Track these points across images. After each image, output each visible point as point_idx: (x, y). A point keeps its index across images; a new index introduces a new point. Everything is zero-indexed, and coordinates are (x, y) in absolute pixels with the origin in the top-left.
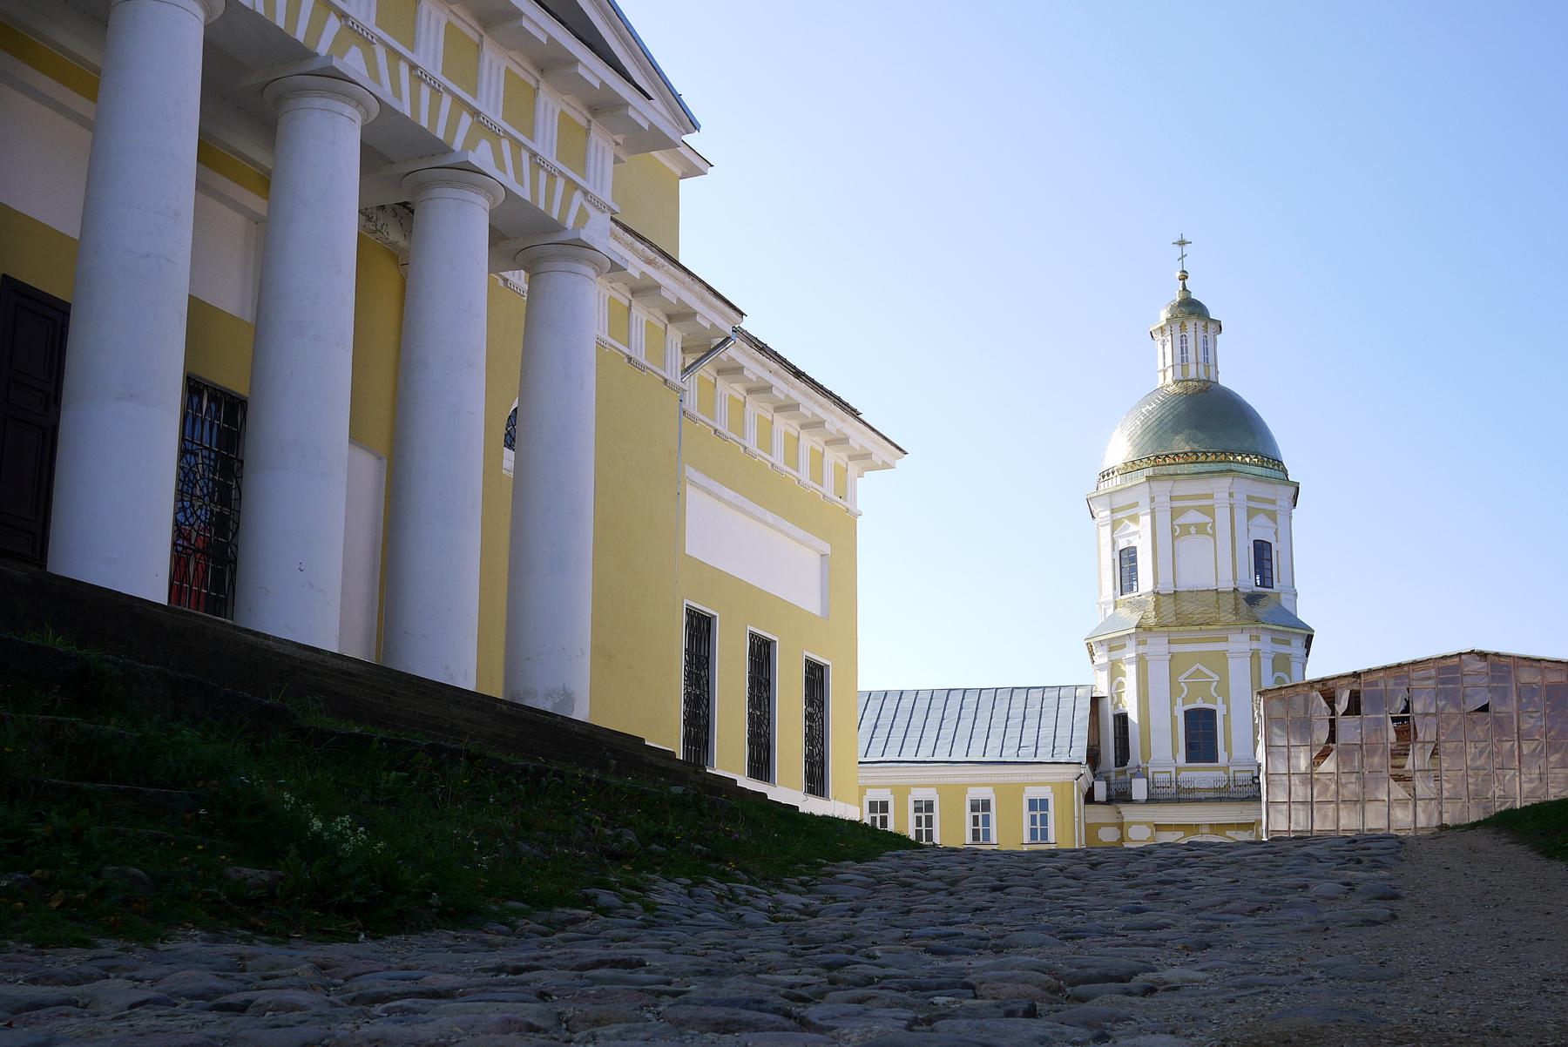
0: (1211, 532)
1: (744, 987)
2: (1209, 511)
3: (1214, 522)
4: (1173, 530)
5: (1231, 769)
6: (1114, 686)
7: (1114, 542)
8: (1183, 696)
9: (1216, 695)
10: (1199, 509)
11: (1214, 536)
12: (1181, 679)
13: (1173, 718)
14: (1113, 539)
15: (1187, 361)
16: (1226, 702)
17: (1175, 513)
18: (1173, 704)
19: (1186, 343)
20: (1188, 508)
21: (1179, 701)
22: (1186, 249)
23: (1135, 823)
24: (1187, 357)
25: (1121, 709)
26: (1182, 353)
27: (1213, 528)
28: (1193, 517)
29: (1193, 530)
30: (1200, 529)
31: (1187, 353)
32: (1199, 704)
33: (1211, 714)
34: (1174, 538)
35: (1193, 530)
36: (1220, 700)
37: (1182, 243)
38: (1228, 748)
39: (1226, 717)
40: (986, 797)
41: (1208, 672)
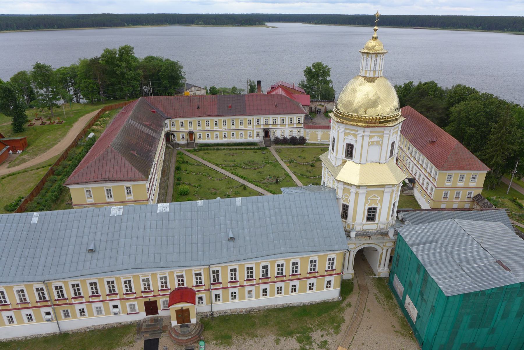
1: (242, 343)
3: (382, 141)
4: (369, 143)
5: (379, 225)
6: (344, 195)
8: (368, 203)
9: (378, 203)
11: (381, 145)
12: (368, 199)
13: (364, 210)
14: (344, 138)
15: (376, 69)
16: (381, 205)
17: (371, 137)
18: (365, 206)
19: (376, 62)
20: (375, 135)
21: (367, 205)
23: (350, 244)
24: (376, 68)
25: (346, 203)
26: (374, 66)
27: (382, 143)
28: (376, 139)
29: (375, 143)
31: (376, 66)
33: (375, 209)
34: (369, 145)
36: (379, 204)
38: (379, 218)
39: (380, 210)
40: (315, 259)
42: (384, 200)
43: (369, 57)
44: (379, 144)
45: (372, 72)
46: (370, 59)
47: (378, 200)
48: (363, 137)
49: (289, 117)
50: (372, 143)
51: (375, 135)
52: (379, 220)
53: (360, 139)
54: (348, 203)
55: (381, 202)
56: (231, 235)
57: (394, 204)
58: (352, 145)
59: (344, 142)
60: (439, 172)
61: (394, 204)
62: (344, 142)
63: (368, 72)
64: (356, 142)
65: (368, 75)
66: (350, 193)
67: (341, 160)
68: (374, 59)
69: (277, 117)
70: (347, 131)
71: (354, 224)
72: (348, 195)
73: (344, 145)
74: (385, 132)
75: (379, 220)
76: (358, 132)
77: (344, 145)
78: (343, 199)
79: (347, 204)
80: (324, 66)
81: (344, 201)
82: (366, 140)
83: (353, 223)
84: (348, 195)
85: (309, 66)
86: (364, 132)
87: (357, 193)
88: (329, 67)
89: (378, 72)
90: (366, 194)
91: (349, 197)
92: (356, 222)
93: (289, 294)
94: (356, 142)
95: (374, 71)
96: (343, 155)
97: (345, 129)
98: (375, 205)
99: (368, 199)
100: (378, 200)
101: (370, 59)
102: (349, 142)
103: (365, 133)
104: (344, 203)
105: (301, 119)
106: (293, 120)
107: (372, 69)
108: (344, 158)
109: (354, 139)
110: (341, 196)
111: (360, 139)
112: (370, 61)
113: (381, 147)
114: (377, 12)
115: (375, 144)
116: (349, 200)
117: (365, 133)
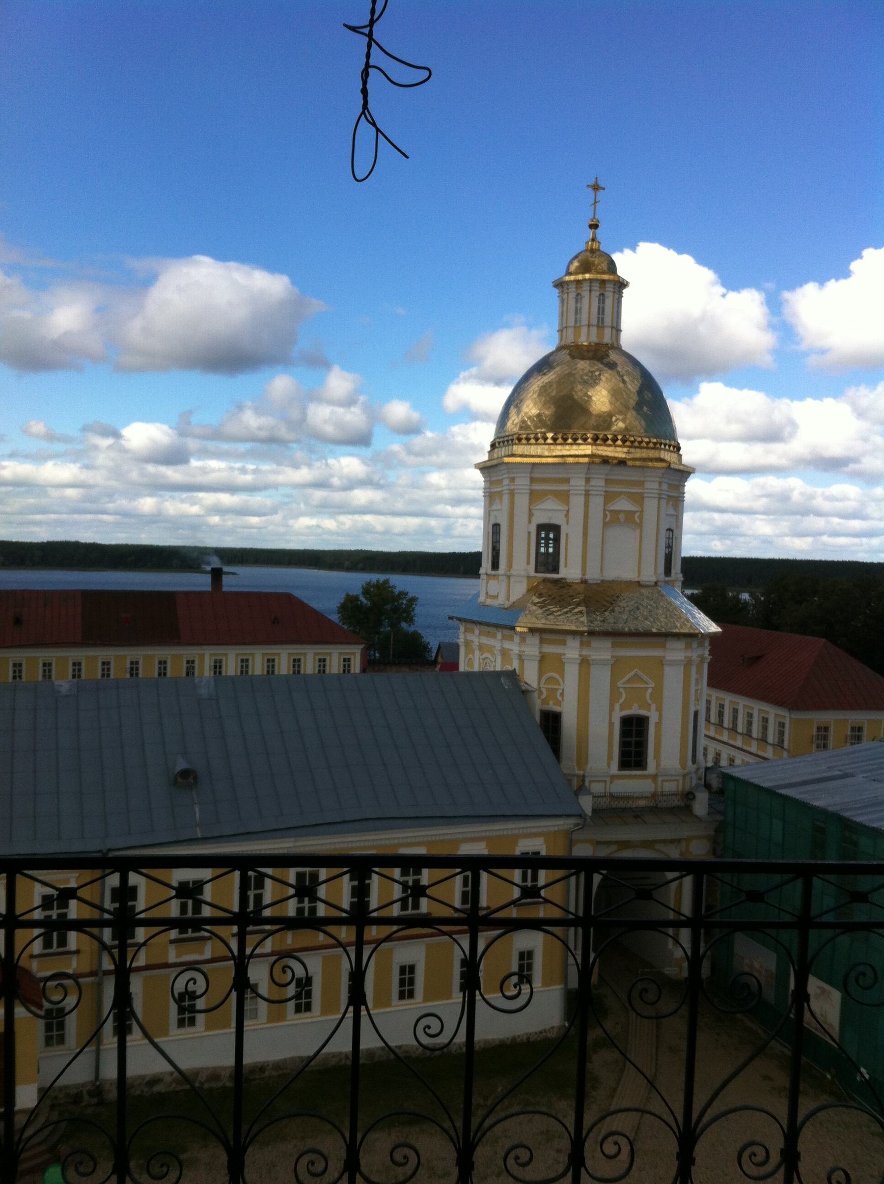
0: (638, 521)
2: (639, 499)
4: (605, 516)
5: (660, 779)
6: (543, 680)
7: (531, 515)
8: (621, 701)
9: (650, 702)
10: (631, 496)
11: (640, 525)
12: (620, 684)
13: (611, 724)
14: (530, 510)
15: (603, 323)
16: (659, 710)
17: (609, 497)
18: (612, 710)
19: (604, 303)
21: (617, 707)
22: (601, 194)
24: (603, 319)
25: (553, 707)
26: (599, 314)
28: (623, 505)
29: (622, 517)
30: (629, 514)
31: (603, 314)
32: (635, 710)
34: (606, 525)
35: (622, 517)
36: (653, 707)
37: (596, 188)
38: (657, 756)
39: (658, 725)
41: (645, 677)
42: (666, 693)
43: (584, 289)
44: (632, 520)
45: (594, 330)
46: (586, 294)
47: (649, 691)
48: (587, 494)
49: (315, 654)
50: (612, 519)
51: (620, 493)
52: (658, 765)
53: (577, 502)
54: (559, 703)
55: (658, 695)
56: (181, 765)
57: (696, 714)
58: (556, 528)
59: (530, 522)
60: (791, 718)
61: (696, 714)
62: (530, 522)
63: (584, 331)
64: (567, 515)
65: (583, 341)
66: (562, 665)
67: (525, 581)
68: (598, 294)
69: (279, 654)
70: (537, 487)
71: (584, 776)
72: (557, 677)
73: (529, 533)
74: (647, 485)
75: (658, 765)
76: (572, 483)
77: (529, 533)
78: (541, 693)
79: (556, 709)
80: (397, 591)
81: (545, 701)
82: (597, 502)
83: (581, 772)
84: (557, 677)
85: (352, 593)
86: (588, 480)
87: (585, 663)
88: (410, 596)
89: (610, 330)
90: (612, 665)
91: (557, 683)
92: (589, 765)
93: (389, 1005)
94: (567, 515)
95: (598, 326)
96: (528, 563)
97: (532, 480)
98: (640, 707)
99: (620, 684)
100: (649, 691)
101: (586, 294)
102: (544, 520)
103: (593, 482)
104: (546, 707)
105: (352, 662)
106: (327, 663)
107: (594, 321)
108: (532, 573)
109: (560, 508)
110: (535, 685)
111: (577, 502)
112: (586, 300)
113: (638, 531)
114: (594, 180)
115: (622, 520)
116: (562, 694)
117: (592, 484)
